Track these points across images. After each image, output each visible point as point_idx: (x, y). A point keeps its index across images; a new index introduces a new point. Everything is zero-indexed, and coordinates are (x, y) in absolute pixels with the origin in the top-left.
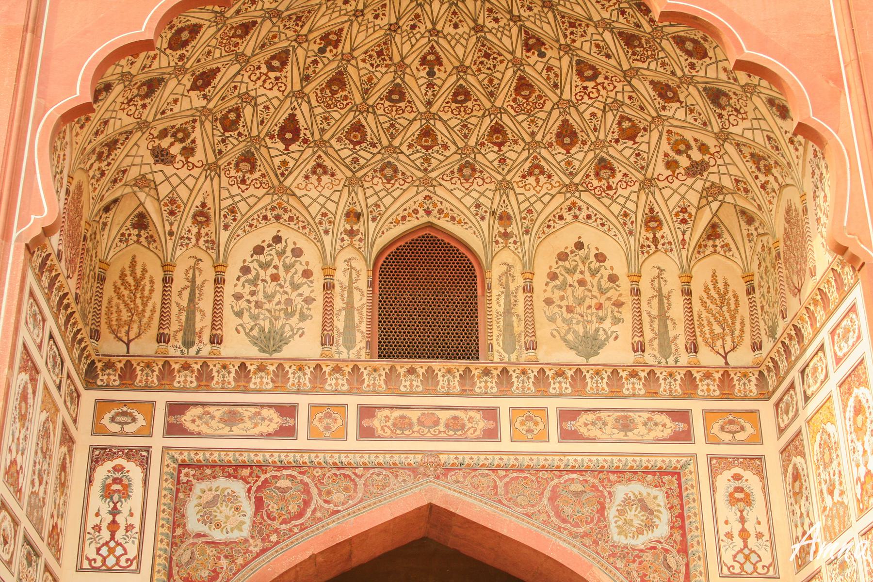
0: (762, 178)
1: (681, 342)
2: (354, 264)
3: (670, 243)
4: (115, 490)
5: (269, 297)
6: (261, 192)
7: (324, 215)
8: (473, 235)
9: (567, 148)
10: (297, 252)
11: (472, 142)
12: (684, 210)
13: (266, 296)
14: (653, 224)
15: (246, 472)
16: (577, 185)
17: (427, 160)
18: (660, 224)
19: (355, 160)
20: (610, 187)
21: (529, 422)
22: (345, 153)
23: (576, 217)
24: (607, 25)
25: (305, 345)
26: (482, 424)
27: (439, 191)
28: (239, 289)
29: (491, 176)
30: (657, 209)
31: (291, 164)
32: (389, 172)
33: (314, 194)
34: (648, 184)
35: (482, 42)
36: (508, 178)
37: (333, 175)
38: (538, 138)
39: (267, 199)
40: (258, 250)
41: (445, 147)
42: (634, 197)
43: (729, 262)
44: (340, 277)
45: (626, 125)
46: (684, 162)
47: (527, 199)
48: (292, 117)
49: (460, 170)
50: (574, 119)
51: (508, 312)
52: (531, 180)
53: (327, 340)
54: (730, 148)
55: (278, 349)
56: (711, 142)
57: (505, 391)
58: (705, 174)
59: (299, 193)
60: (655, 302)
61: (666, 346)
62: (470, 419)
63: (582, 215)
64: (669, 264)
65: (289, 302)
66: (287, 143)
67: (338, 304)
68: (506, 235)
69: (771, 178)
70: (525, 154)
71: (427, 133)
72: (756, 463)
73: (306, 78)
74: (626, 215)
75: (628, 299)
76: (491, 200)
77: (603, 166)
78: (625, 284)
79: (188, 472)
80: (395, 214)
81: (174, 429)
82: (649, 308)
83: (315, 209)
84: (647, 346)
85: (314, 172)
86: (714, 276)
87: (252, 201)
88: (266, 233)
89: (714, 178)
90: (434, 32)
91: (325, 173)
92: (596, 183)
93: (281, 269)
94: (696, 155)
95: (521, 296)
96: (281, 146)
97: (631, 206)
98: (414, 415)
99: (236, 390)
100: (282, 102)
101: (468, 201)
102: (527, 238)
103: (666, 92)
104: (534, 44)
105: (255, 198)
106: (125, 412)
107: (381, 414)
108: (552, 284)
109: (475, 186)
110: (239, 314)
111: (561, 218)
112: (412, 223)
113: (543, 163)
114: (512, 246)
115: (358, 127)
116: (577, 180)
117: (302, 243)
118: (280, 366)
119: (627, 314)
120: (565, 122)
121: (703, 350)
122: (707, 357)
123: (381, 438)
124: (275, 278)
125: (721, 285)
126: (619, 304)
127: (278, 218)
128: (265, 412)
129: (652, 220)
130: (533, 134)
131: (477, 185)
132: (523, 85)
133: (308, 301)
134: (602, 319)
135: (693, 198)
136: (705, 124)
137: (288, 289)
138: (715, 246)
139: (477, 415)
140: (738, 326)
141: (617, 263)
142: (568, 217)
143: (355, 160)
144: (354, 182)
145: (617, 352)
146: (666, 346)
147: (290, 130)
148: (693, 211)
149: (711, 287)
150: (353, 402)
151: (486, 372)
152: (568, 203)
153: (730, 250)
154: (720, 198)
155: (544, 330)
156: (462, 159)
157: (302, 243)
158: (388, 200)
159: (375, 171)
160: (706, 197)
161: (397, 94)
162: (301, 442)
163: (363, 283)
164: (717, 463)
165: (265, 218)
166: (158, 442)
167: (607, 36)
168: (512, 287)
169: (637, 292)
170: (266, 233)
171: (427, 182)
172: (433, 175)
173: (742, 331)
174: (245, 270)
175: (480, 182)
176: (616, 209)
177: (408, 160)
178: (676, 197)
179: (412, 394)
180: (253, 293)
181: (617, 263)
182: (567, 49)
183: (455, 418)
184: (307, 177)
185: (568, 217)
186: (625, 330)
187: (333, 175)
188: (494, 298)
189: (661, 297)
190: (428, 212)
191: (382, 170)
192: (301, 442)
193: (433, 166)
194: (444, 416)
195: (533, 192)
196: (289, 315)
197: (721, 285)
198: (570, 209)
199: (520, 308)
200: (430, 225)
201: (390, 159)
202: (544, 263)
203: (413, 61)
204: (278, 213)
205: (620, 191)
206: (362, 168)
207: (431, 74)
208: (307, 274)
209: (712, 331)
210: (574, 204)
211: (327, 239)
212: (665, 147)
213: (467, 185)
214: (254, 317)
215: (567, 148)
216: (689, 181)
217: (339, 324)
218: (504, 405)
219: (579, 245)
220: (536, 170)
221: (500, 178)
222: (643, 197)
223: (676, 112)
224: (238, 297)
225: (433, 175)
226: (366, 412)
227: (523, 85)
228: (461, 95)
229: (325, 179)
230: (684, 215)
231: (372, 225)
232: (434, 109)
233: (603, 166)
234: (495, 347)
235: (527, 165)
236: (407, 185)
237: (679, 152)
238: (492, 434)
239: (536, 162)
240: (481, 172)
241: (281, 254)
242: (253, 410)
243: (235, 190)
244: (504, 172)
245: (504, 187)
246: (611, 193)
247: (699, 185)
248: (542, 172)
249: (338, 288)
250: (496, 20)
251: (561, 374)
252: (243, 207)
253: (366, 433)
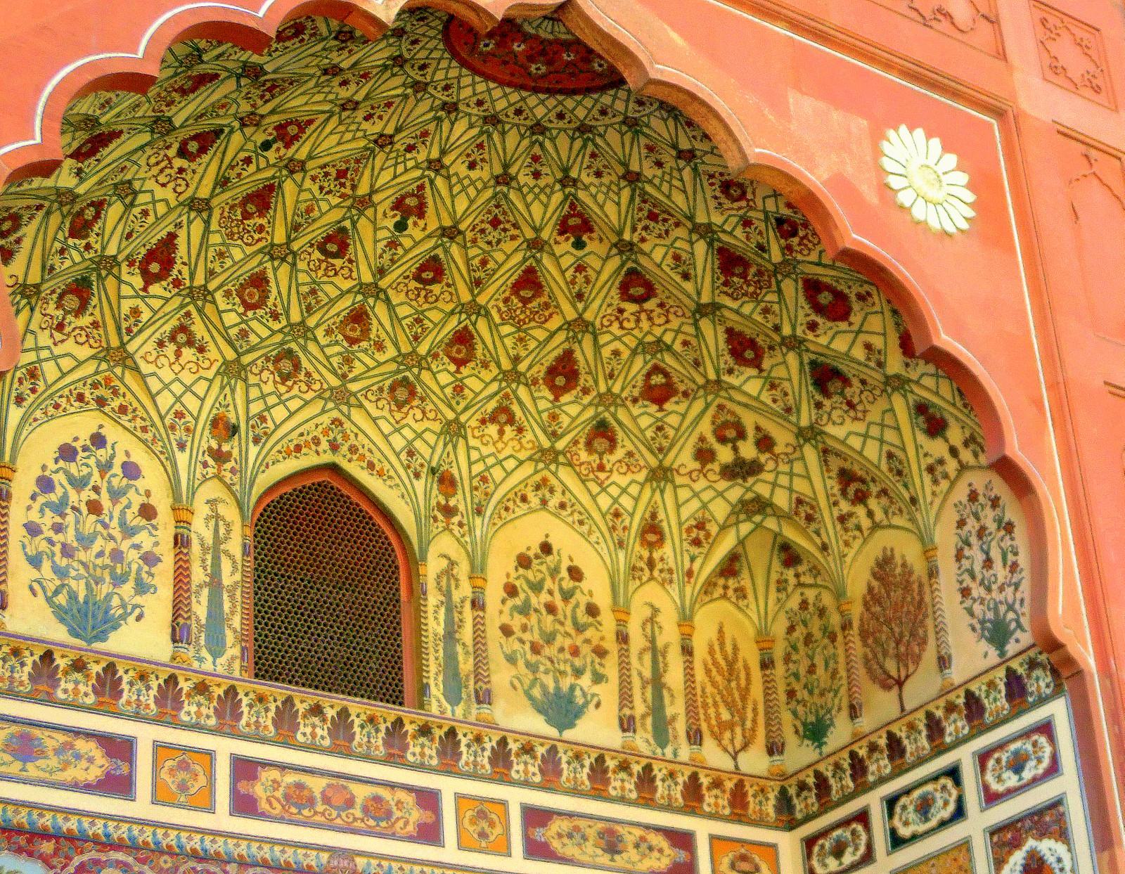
0: (845, 506)
1: (681, 726)
2: (222, 509)
3: (670, 571)
5: (86, 541)
6: (84, 352)
7: (179, 415)
8: (403, 499)
9: (558, 392)
10: (131, 471)
11: (423, 349)
12: (700, 526)
13: (80, 538)
14: (652, 537)
15: (47, 847)
16: (557, 453)
17: (348, 361)
18: (661, 540)
19: (244, 334)
20: (601, 468)
22: (230, 319)
23: (544, 502)
24: (706, 232)
25: (143, 637)
26: (416, 815)
27: (356, 415)
28: (34, 516)
29: (438, 410)
30: (661, 516)
31: (145, 316)
32: (287, 365)
33: (167, 375)
34: (661, 475)
35: (498, 201)
36: (463, 418)
37: (201, 350)
38: (522, 367)
39: (90, 368)
40: (67, 453)
41: (380, 347)
42: (634, 490)
43: (740, 616)
44: (200, 529)
45: (658, 379)
46: (725, 455)
47: (483, 458)
48: (169, 241)
49: (392, 389)
50: (584, 353)
51: (450, 636)
52: (492, 429)
53: (178, 634)
54: (811, 454)
55: (102, 636)
56: (783, 438)
57: (448, 765)
58: (751, 480)
59: (146, 368)
60: (648, 658)
62: (399, 803)
63: (553, 502)
65: (117, 555)
66: (149, 279)
67: (198, 575)
68: (449, 511)
69: (860, 511)
70: (494, 387)
71: (359, 317)
73: (223, 183)
74: (617, 515)
75: (611, 645)
76: (430, 450)
77: (602, 433)
78: (608, 622)
82: (641, 667)
83: (165, 401)
84: (638, 724)
85: (173, 339)
86: (721, 631)
87: (66, 364)
88: (81, 425)
89: (763, 490)
90: (436, 165)
91: (190, 343)
92: (584, 456)
93: (104, 492)
94: (748, 450)
95: (468, 614)
96: (138, 282)
97: (626, 502)
98: (317, 785)
99: (31, 698)
100: (170, 210)
101: (398, 442)
102: (478, 521)
103: (744, 349)
104: (577, 226)
107: (268, 775)
108: (510, 603)
109: (409, 420)
110: (35, 561)
111: (524, 499)
112: (309, 460)
113: (516, 408)
114: (456, 529)
115: (259, 281)
116: (560, 445)
117: (140, 456)
118: (111, 669)
119: (611, 668)
120: (568, 354)
121: (709, 743)
122: (714, 755)
123: (263, 816)
124: (94, 507)
125: (729, 648)
126: (601, 653)
127: (101, 402)
128: (82, 745)
129: (652, 531)
130: (516, 360)
131: (412, 418)
132: (529, 282)
133: (150, 559)
134: (578, 673)
135: (720, 510)
136: (788, 410)
137: (116, 533)
138: (726, 587)
139: (409, 799)
140: (750, 715)
141: (596, 587)
142: (534, 501)
143: (244, 334)
144: (234, 370)
145: (597, 729)
147: (158, 261)
148: (713, 529)
149: (717, 648)
150: (225, 748)
151: (425, 731)
152: (538, 478)
153: (745, 597)
154: (757, 518)
155: (501, 676)
156: (398, 372)
157: (140, 456)
158: (279, 413)
159: (268, 359)
160: (737, 514)
161: (337, 244)
162: (141, 806)
163: (235, 546)
165: (80, 398)
167: (701, 247)
168: (456, 596)
169: (623, 638)
170: (81, 425)
171: (341, 396)
172: (354, 387)
173: (754, 721)
174: (45, 484)
175: (419, 416)
176: (605, 502)
177: (321, 355)
178: (695, 504)
179: (311, 748)
180: (58, 528)
181: (596, 587)
182: (625, 248)
183: (377, 799)
184: (161, 344)
185: (534, 501)
186: (608, 693)
187: (201, 350)
188: (430, 609)
189: (656, 652)
190: (334, 447)
191: (277, 359)
192: (141, 806)
193: (356, 372)
194: (361, 793)
195: (491, 449)
196: (119, 580)
197: (729, 648)
198: (538, 488)
199: (467, 634)
200: (334, 468)
201: (293, 346)
202: (500, 569)
203: (384, 201)
205: (615, 477)
206: (252, 349)
207: (401, 226)
208: (147, 512)
209: (718, 715)
210: (545, 480)
211: (182, 459)
212: (706, 427)
213: (398, 416)
214: (61, 572)
215: (558, 392)
216: (722, 485)
217: (200, 609)
218: (448, 787)
219: (546, 548)
220: (503, 415)
221: (450, 415)
222: (647, 493)
223: (749, 383)
224: (33, 530)
225: (354, 387)
226: (244, 769)
227: (529, 282)
228: (431, 271)
229: (188, 353)
230: (699, 533)
231: (253, 450)
232: (383, 283)
233: (602, 433)
234: (434, 690)
235: (492, 405)
236: (308, 396)
237: (722, 440)
238: (430, 833)
239: (505, 403)
240: (423, 400)
241: (105, 468)
242: (61, 738)
243: (44, 339)
244: (460, 408)
245: (454, 431)
246: (602, 476)
247: (735, 493)
248: (511, 420)
249: (196, 548)
250: (537, 175)
251: (528, 750)
252: (50, 371)
253: (244, 805)
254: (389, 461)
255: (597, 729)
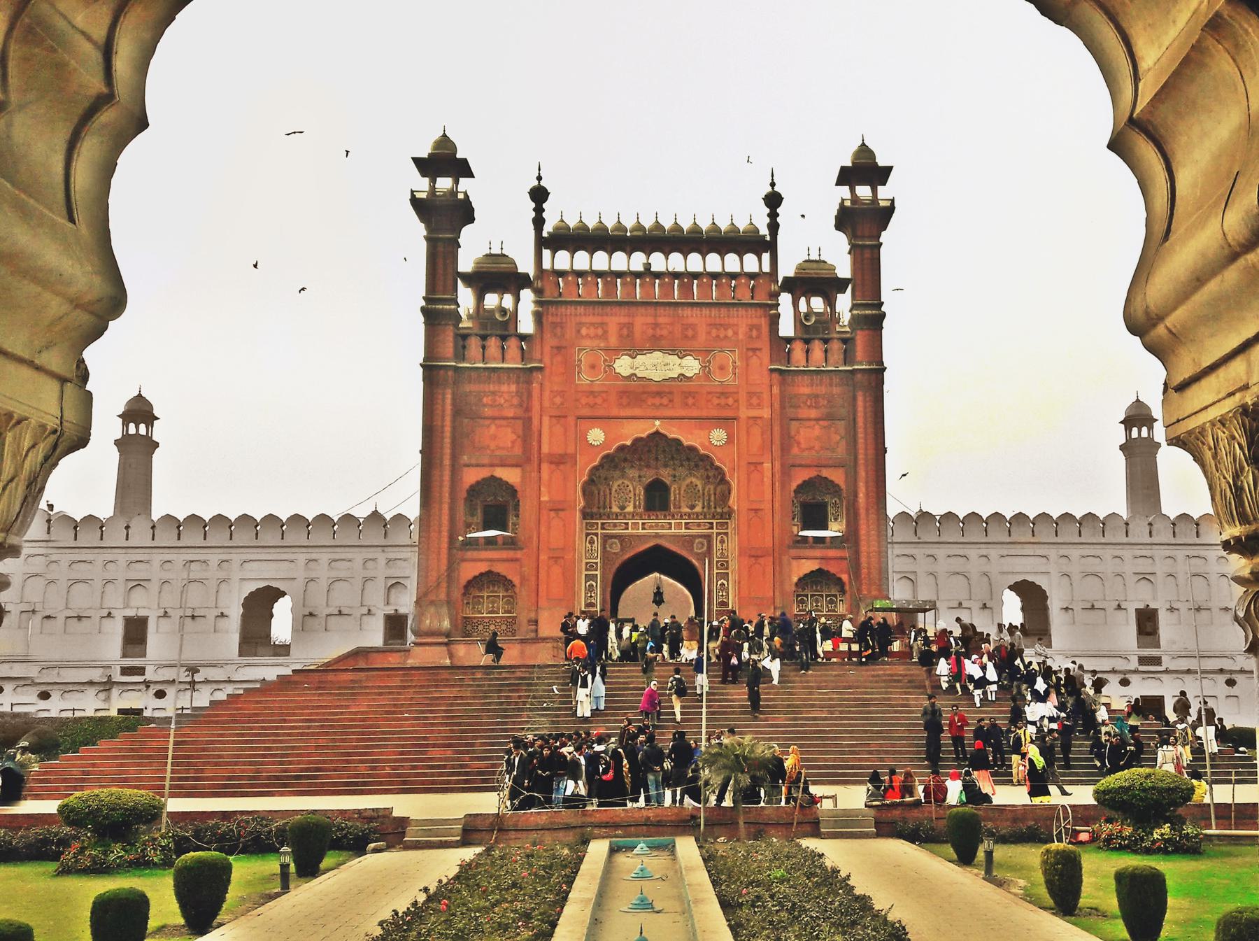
4: (592, 542)
8: (667, 481)
21: (679, 526)
25: (630, 509)
32: (648, 466)
53: (635, 507)
57: (673, 518)
61: (709, 507)
64: (712, 487)
72: (726, 534)
79: (606, 538)
80: (649, 476)
81: (603, 528)
105: (617, 473)
106: (592, 525)
129: (708, 477)
141: (700, 487)
145: (698, 509)
146: (709, 507)
162: (630, 531)
164: (718, 534)
166: (599, 531)
170: (620, 482)
171: (657, 468)
186: (700, 504)
189: (709, 495)
192: (630, 531)
204: (623, 477)
220: (682, 465)
233: (697, 466)
254: (665, 475)
255: (698, 509)
